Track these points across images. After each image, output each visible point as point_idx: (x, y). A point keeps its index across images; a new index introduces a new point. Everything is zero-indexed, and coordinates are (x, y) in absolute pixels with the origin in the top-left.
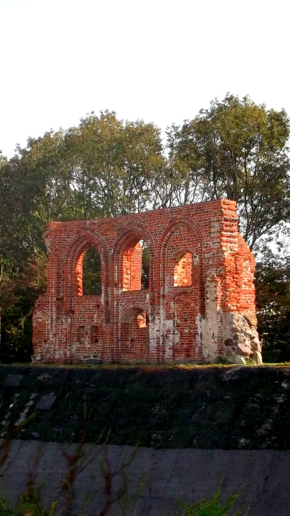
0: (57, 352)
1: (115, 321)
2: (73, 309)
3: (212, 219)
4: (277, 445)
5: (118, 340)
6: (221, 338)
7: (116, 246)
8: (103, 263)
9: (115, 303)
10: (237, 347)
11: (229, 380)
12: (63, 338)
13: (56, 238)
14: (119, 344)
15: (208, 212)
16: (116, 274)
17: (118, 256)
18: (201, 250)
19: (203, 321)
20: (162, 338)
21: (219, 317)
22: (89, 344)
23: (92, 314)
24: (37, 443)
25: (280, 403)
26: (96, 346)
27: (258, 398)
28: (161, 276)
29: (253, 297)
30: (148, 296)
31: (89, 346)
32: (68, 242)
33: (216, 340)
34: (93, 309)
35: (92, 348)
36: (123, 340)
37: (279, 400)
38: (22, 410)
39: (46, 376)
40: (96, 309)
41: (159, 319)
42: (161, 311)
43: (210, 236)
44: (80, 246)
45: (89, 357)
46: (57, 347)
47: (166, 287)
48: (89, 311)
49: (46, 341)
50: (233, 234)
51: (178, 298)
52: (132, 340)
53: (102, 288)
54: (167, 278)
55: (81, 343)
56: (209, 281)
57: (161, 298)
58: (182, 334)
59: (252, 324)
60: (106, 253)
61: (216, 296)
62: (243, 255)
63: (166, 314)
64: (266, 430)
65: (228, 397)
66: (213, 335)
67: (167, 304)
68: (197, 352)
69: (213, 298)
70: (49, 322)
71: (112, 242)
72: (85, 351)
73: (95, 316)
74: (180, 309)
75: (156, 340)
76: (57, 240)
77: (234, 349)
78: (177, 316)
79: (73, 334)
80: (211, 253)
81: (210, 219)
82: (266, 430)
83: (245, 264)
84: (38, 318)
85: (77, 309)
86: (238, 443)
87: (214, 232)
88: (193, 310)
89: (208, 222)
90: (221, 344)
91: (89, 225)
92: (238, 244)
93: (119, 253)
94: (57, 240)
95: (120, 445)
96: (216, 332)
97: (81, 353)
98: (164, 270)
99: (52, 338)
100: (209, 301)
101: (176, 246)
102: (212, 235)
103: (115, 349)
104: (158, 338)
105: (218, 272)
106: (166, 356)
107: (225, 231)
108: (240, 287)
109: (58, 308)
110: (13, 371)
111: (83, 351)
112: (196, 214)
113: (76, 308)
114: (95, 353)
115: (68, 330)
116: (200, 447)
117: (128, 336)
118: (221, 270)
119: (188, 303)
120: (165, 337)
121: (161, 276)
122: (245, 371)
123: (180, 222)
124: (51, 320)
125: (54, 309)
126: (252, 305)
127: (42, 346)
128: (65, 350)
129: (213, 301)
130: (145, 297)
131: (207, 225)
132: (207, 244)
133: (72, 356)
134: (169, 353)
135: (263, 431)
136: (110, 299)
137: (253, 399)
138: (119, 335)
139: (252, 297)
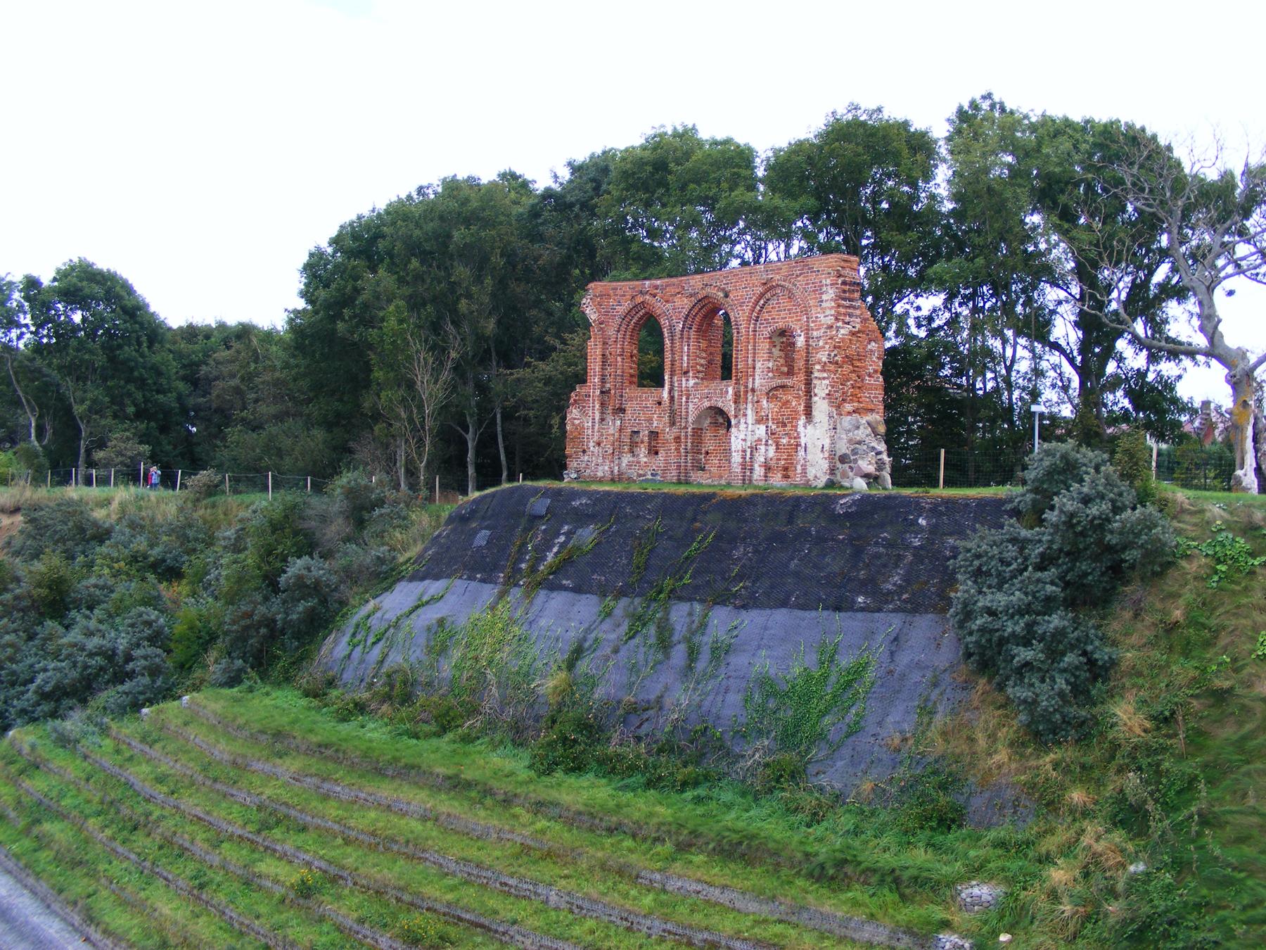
0: (600, 468)
1: (683, 425)
3: (824, 282)
4: (909, 606)
7: (686, 318)
8: (667, 342)
9: (684, 399)
14: (689, 458)
16: (685, 358)
18: (808, 326)
19: (809, 427)
20: (749, 450)
24: (571, 595)
25: (915, 547)
27: (885, 538)
28: (750, 362)
29: (879, 395)
30: (730, 390)
31: (645, 460)
33: (827, 455)
38: (549, 549)
42: (749, 412)
44: (636, 318)
45: (644, 475)
46: (600, 460)
47: (757, 377)
49: (584, 452)
52: (707, 453)
53: (666, 378)
54: (758, 365)
55: (634, 456)
56: (818, 371)
57: (750, 394)
58: (777, 445)
60: (671, 327)
64: (895, 584)
67: (758, 402)
68: (799, 471)
70: (590, 424)
71: (680, 312)
75: (740, 453)
77: (850, 467)
78: (773, 419)
82: (895, 584)
83: (869, 347)
86: (854, 602)
88: (796, 412)
96: (827, 442)
98: (754, 353)
102: (824, 305)
104: (744, 451)
106: (755, 477)
107: (844, 299)
108: (862, 380)
109: (602, 404)
110: (536, 491)
112: (801, 274)
113: (628, 406)
115: (617, 435)
118: (836, 355)
119: (788, 401)
120: (754, 449)
121: (750, 362)
122: (865, 499)
123: (778, 285)
125: (597, 406)
130: (727, 392)
133: (621, 473)
134: (759, 472)
135: (890, 587)
136: (676, 394)
138: (689, 444)
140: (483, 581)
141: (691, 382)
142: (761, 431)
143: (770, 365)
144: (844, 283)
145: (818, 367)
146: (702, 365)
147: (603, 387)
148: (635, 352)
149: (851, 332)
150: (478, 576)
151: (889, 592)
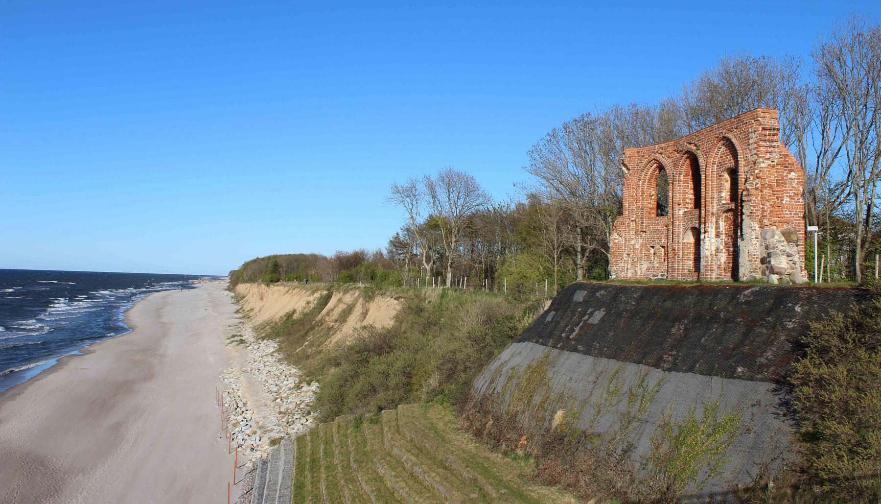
2: (644, 230)
3: (750, 130)
5: (680, 260)
6: (756, 256)
10: (770, 265)
11: (745, 301)
12: (635, 258)
13: (630, 163)
15: (747, 123)
17: (679, 176)
20: (709, 256)
21: (754, 234)
22: (658, 263)
23: (661, 234)
26: (664, 265)
31: (657, 265)
32: (640, 167)
34: (661, 230)
35: (660, 267)
36: (685, 260)
37: (789, 325)
39: (602, 293)
40: (664, 230)
41: (708, 237)
43: (748, 148)
44: (651, 170)
45: (657, 276)
46: (629, 266)
47: (715, 204)
48: (658, 232)
50: (773, 144)
51: (725, 216)
56: (746, 196)
59: (790, 241)
61: (750, 211)
62: (788, 167)
63: (716, 232)
65: (739, 320)
66: (748, 253)
69: (749, 214)
70: (624, 242)
72: (654, 270)
73: (663, 235)
74: (727, 227)
76: (632, 166)
78: (726, 234)
79: (645, 254)
80: (749, 166)
81: (748, 131)
82: (767, 359)
83: (789, 176)
84: (615, 239)
85: (648, 230)
86: (735, 371)
87: (752, 144)
89: (747, 134)
90: (756, 263)
91: (658, 149)
92: (780, 155)
93: (682, 174)
94: (632, 166)
95: (637, 364)
97: (651, 271)
99: (626, 257)
101: (724, 162)
102: (751, 147)
103: (676, 268)
105: (754, 185)
111: (652, 271)
114: (662, 272)
115: (639, 250)
116: (702, 373)
117: (690, 255)
124: (625, 241)
126: (799, 220)
127: (618, 265)
128: (637, 269)
129: (748, 216)
131: (746, 137)
132: (747, 157)
135: (763, 360)
137: (762, 323)
138: (681, 254)
139: (799, 212)
140: (543, 344)
144: (764, 129)
146: (691, 199)
148: (653, 193)
149: (769, 165)
150: (540, 341)
151: (762, 366)
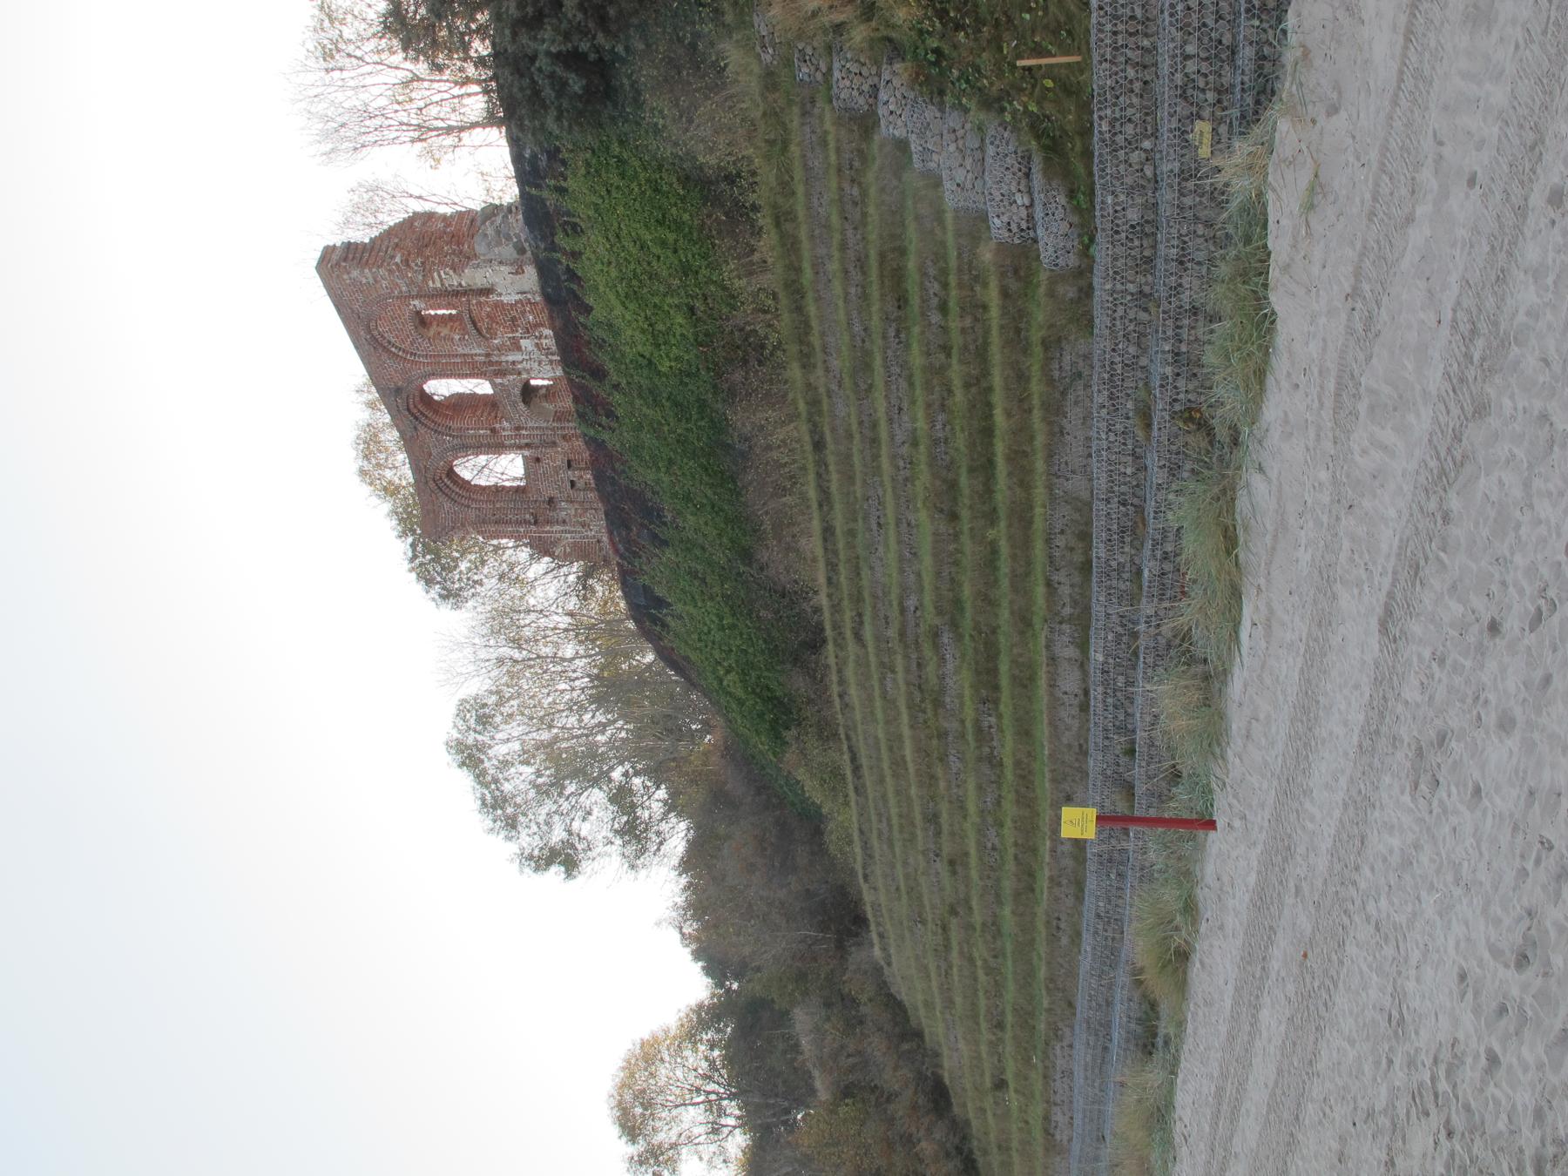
9: (524, 432)
42: (510, 358)
44: (454, 488)
47: (473, 352)
49: (599, 541)
54: (460, 351)
58: (537, 325)
78: (513, 332)
100: (463, 283)
109: (548, 522)
119: (488, 316)
125: (548, 528)
141: (506, 424)
142: (526, 344)
143: (457, 337)
144: (345, 260)
145: (430, 283)
147: (530, 523)
